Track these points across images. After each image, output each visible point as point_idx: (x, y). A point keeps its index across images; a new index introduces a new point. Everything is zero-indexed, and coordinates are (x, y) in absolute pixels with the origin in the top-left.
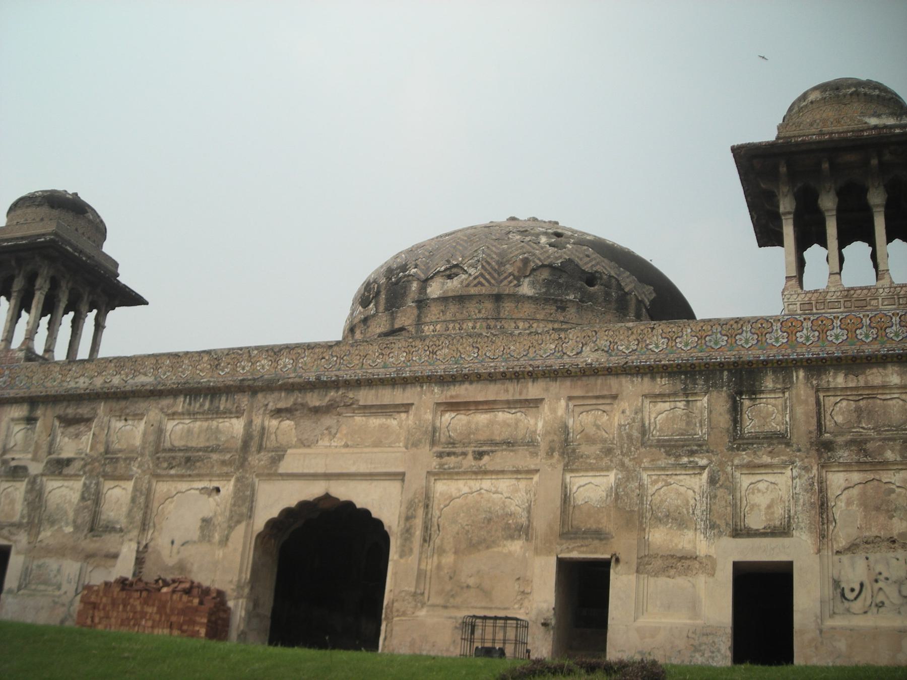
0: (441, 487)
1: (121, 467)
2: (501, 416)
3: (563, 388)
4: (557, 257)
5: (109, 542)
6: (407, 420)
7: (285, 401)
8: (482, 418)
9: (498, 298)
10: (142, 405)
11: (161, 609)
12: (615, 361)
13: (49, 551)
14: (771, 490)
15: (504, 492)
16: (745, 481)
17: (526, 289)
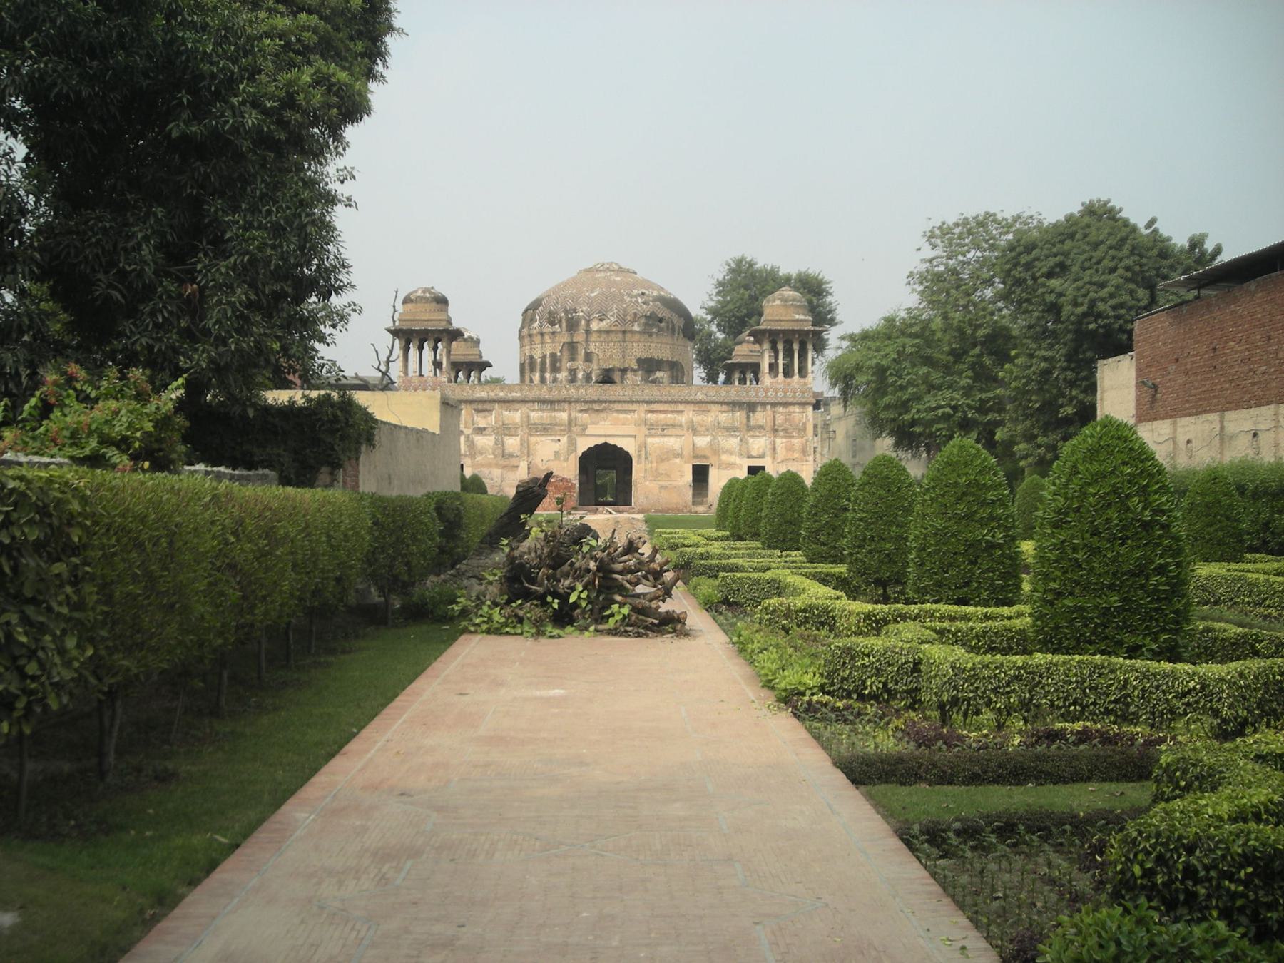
0: (649, 440)
1: (513, 431)
2: (669, 415)
3: (691, 407)
4: (647, 310)
5: (514, 461)
6: (636, 416)
7: (586, 407)
8: (662, 416)
9: (624, 332)
10: (517, 406)
11: (556, 487)
12: (710, 399)
13: (482, 465)
14: (759, 443)
15: (673, 442)
16: (751, 440)
17: (636, 328)
